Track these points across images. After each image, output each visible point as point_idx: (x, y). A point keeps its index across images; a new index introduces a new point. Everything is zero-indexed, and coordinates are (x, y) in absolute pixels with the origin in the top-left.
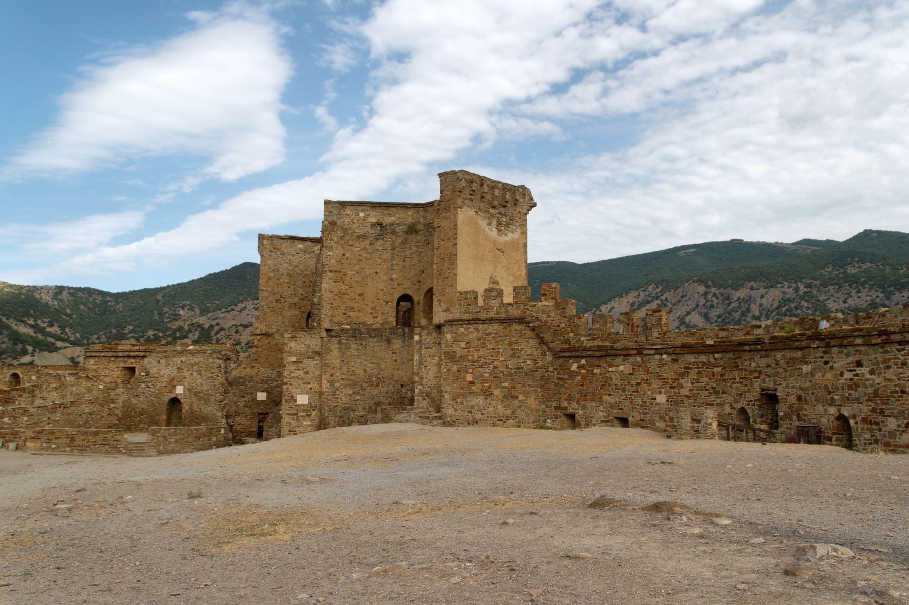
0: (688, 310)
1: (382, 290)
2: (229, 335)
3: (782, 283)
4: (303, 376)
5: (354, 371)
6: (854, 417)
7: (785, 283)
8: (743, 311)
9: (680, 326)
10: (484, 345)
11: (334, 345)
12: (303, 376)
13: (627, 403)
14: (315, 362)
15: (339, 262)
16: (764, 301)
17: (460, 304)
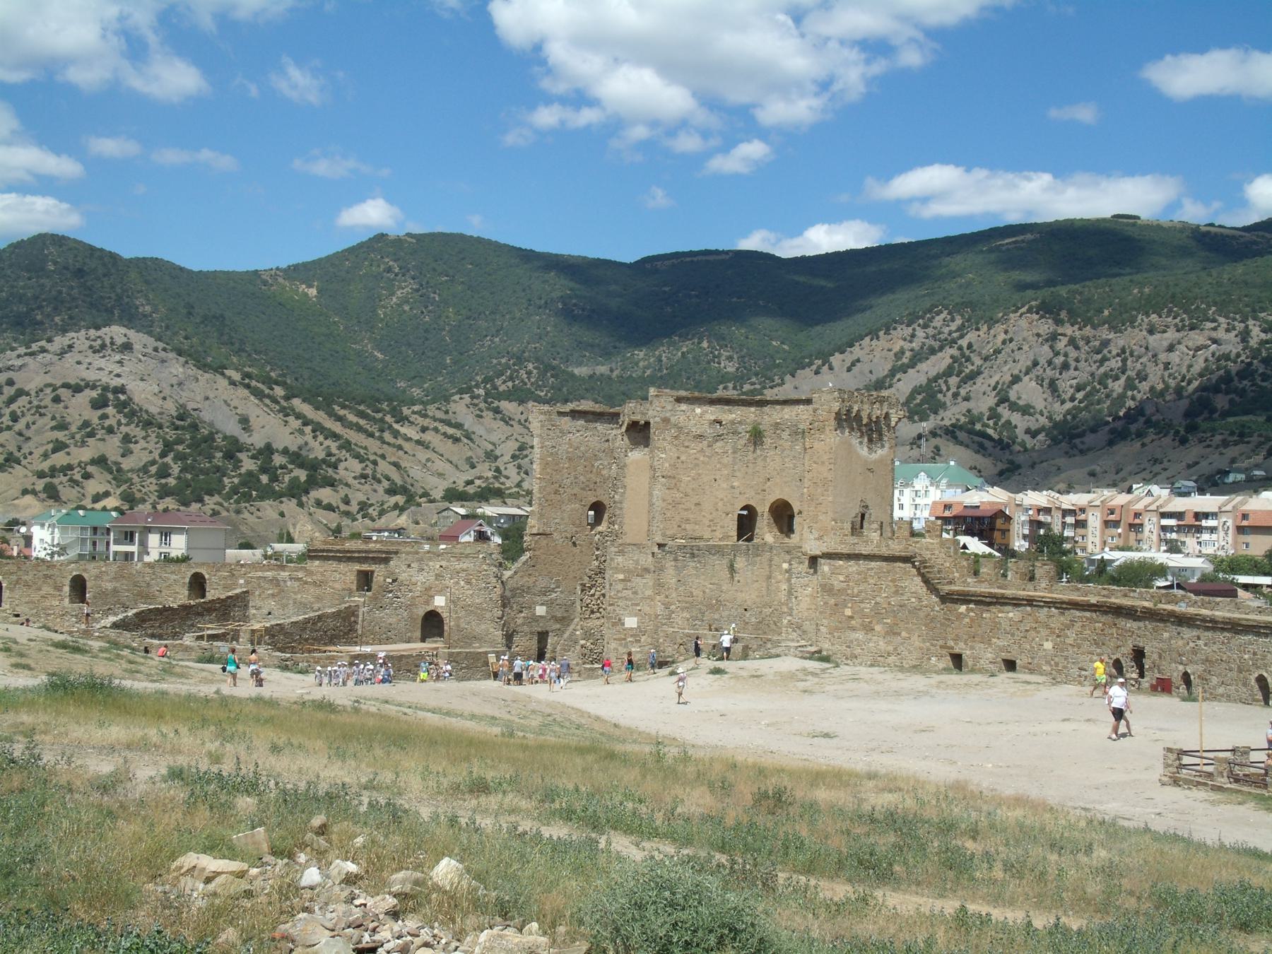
0: (1016, 372)
1: (722, 500)
2: (39, 407)
3: (1214, 321)
4: (632, 596)
5: (691, 593)
6: (1194, 674)
7: (1222, 320)
8: (1128, 378)
9: (997, 405)
10: (865, 580)
11: (669, 564)
12: (632, 596)
13: (1016, 647)
14: (645, 581)
15: (674, 466)
16: (1174, 357)
17: (835, 534)
